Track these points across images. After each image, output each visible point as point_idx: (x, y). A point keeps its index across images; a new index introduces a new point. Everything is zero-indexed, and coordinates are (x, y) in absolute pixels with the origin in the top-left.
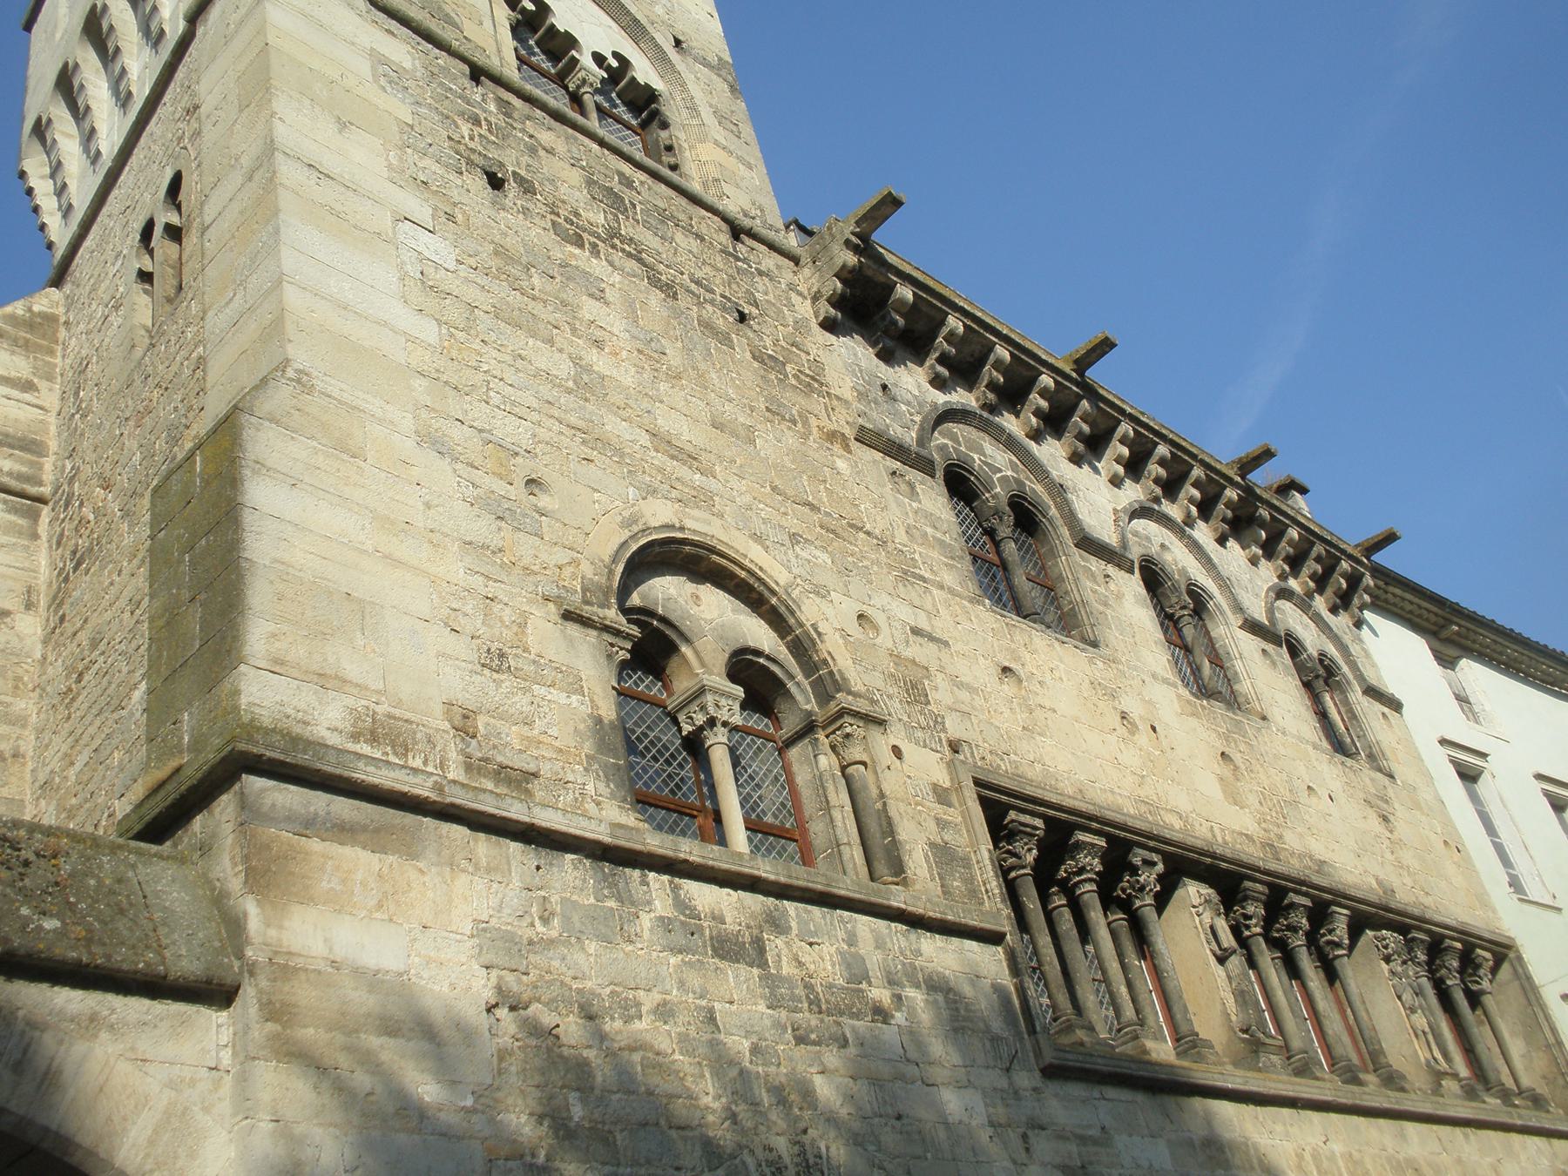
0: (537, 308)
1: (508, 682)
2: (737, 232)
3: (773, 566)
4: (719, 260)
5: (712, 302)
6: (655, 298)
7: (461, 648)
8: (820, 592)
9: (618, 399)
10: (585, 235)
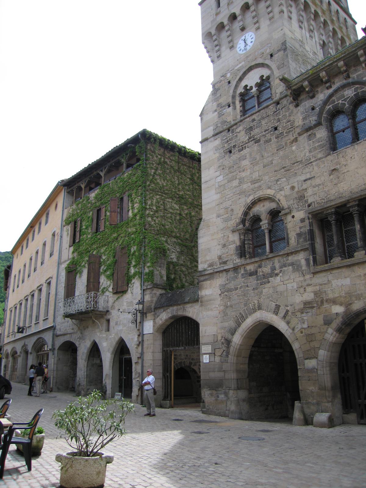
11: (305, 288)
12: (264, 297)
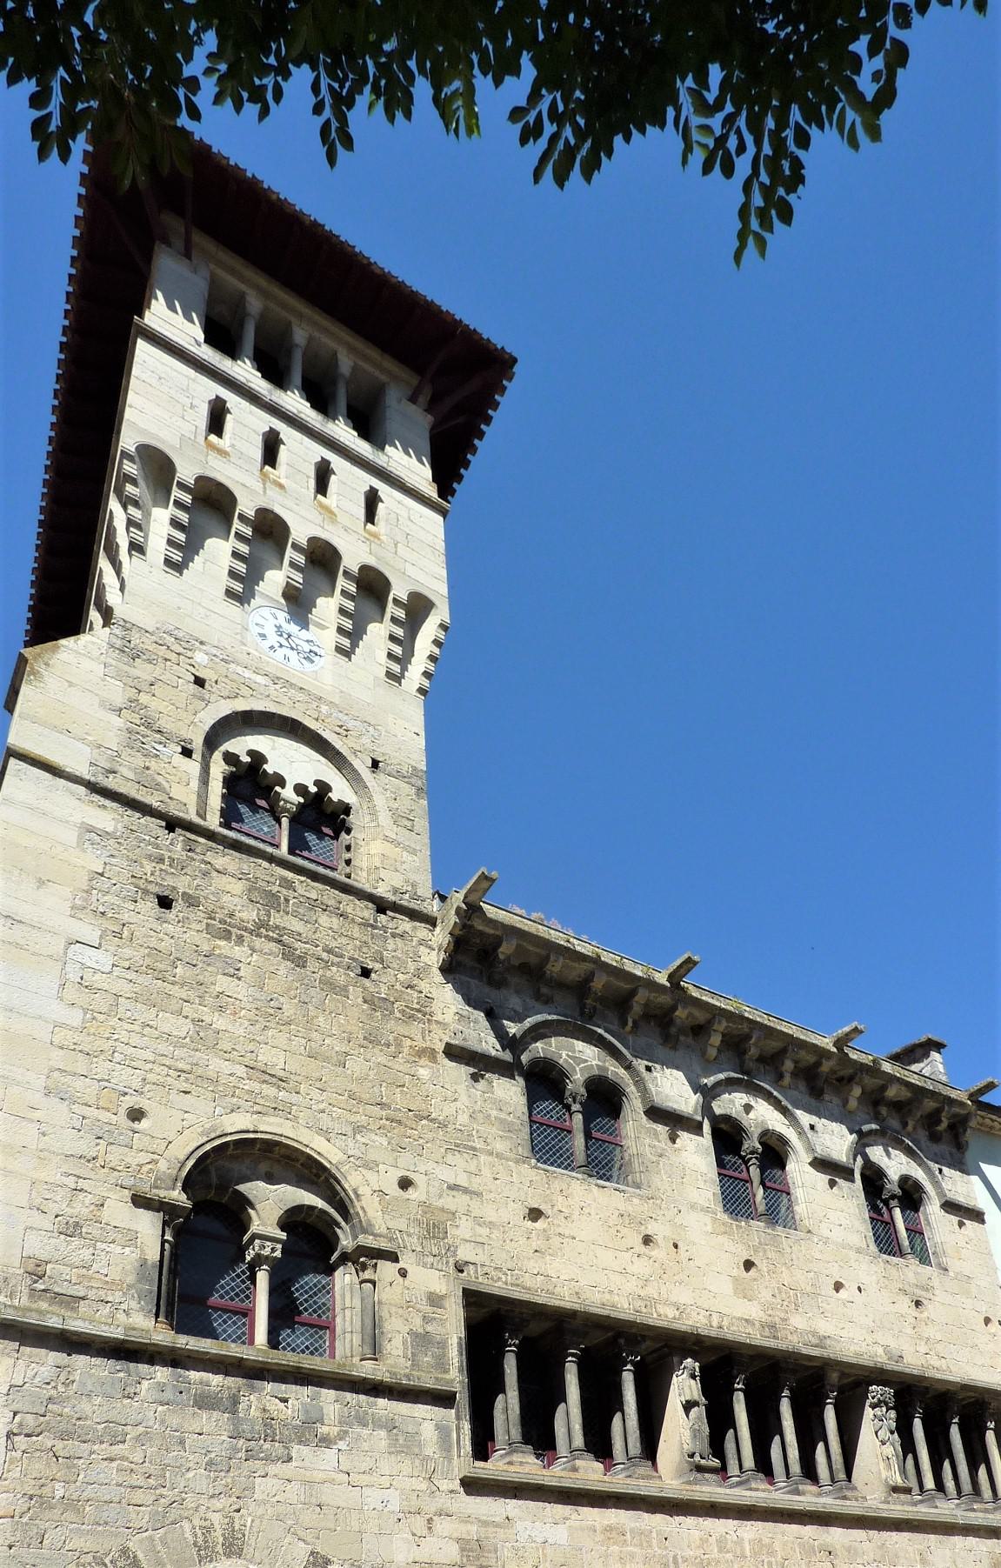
0: (176, 991)
1: (76, 1242)
2: (382, 906)
3: (327, 1151)
4: (356, 932)
5: (338, 965)
6: (284, 967)
7: (46, 1222)
8: (370, 1165)
9: (227, 1046)
10: (234, 930)
11: (430, 1521)
12: (260, 1511)
